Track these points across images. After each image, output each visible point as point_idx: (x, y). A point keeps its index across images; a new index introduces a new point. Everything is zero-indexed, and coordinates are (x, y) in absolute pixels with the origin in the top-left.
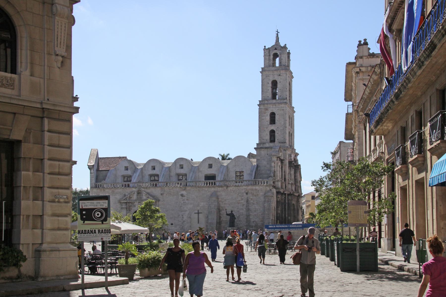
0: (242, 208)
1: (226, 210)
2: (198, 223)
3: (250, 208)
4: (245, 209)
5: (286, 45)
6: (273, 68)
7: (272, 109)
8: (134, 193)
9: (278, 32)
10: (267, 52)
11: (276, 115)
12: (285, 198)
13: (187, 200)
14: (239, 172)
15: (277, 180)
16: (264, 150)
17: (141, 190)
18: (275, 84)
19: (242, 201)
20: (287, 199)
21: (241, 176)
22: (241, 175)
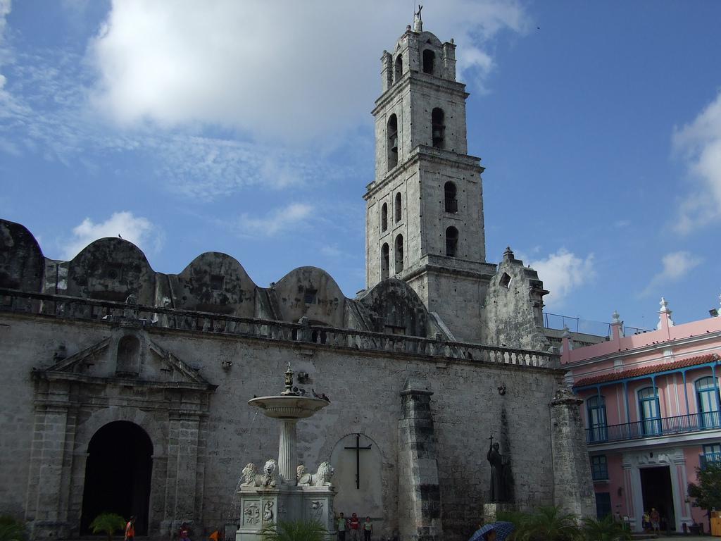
2: (358, 488)
5: (453, 40)
16: (449, 275)
18: (438, 115)
19: (490, 416)
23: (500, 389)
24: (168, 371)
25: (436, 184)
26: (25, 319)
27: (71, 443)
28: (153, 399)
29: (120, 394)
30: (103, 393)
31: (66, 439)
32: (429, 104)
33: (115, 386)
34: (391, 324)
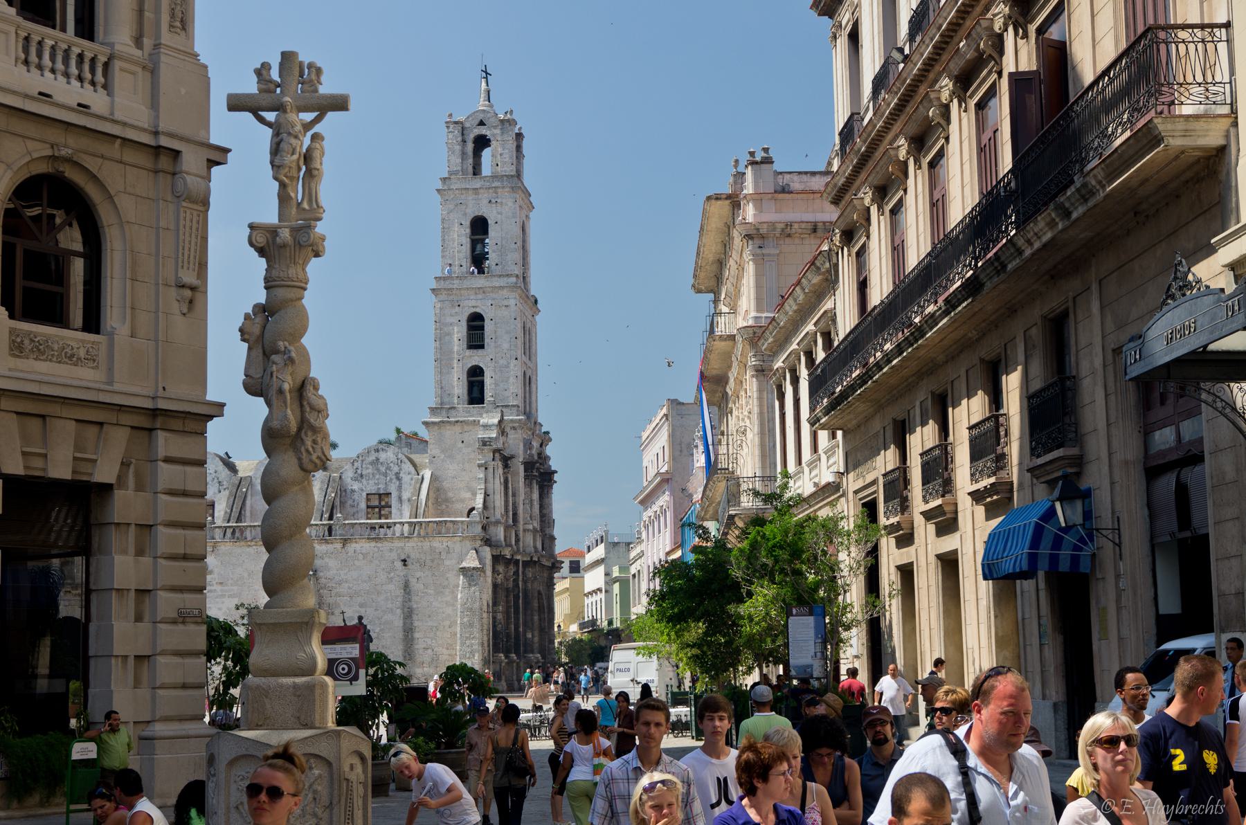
0: (390, 606)
1: (343, 613)
3: (415, 606)
4: (399, 611)
6: (477, 183)
7: (473, 303)
9: (487, 73)
10: (456, 132)
11: (486, 321)
12: (516, 573)
13: (221, 583)
14: (377, 497)
15: (492, 519)
19: (391, 587)
20: (521, 578)
21: (383, 507)
22: (383, 503)
23: (402, 561)
25: (454, 320)
32: (465, 214)
34: (373, 492)
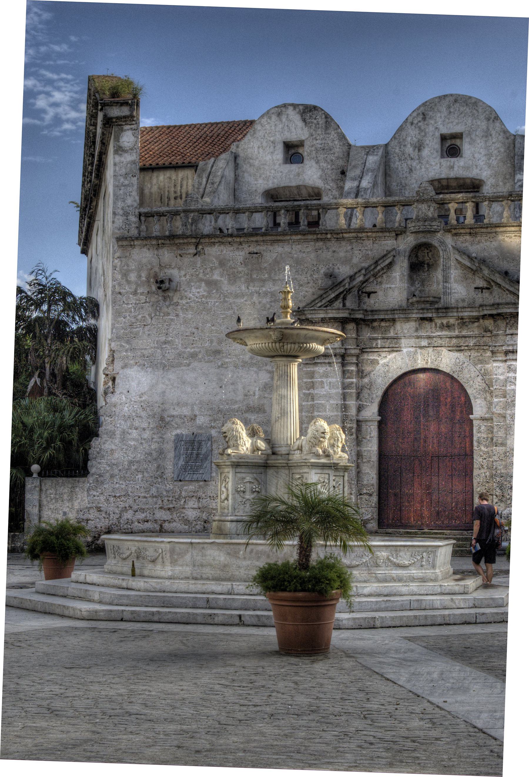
8: (390, 265)
17: (435, 243)
24: (488, 288)
26: (278, 241)
27: (352, 403)
28: (464, 333)
29: (417, 330)
30: (392, 331)
31: (344, 399)
33: (408, 320)
